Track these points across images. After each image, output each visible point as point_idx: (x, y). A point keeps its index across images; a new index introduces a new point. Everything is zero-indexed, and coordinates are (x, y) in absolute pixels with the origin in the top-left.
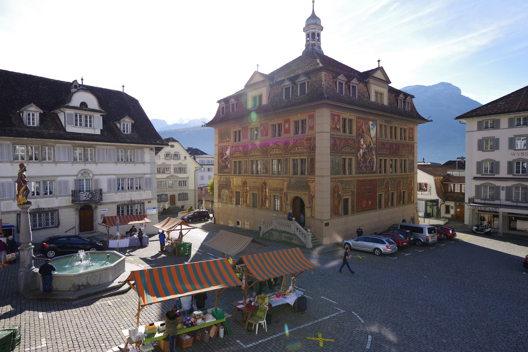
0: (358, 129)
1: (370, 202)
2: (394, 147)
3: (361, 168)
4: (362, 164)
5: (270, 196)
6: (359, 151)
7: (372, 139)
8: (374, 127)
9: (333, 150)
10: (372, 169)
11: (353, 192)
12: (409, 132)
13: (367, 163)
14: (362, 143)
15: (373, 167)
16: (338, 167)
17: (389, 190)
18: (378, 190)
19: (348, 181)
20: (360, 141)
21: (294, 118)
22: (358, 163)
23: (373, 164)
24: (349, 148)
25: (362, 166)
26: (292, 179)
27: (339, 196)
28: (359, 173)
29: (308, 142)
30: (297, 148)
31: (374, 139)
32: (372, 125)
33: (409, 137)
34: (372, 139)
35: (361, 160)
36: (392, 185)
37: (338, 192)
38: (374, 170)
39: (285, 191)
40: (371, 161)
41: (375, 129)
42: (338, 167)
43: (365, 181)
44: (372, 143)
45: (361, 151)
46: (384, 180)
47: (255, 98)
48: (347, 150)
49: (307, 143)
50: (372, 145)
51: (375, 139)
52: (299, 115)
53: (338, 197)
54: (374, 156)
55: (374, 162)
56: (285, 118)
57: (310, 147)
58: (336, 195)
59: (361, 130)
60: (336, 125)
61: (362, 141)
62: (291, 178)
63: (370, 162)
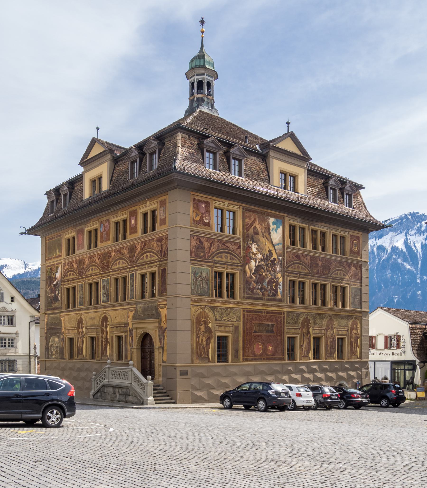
0: (246, 227)
1: (270, 348)
2: (320, 263)
4: (253, 285)
5: (112, 337)
6: (248, 262)
7: (273, 245)
8: (278, 227)
9: (197, 256)
10: (275, 294)
11: (237, 328)
12: (352, 243)
14: (254, 250)
15: (276, 291)
16: (207, 284)
17: (308, 333)
18: (286, 330)
19: (227, 309)
20: (249, 248)
21: (142, 209)
22: (247, 282)
23: (276, 286)
24: (229, 255)
26: (138, 306)
27: (208, 330)
28: (249, 298)
29: (159, 243)
30: (145, 255)
32: (274, 223)
33: (352, 251)
34: (273, 245)
35: (251, 277)
37: (206, 323)
38: (279, 296)
39: (130, 326)
40: (273, 282)
41: (280, 230)
42: (207, 284)
43: (260, 311)
44: (273, 252)
46: (299, 315)
47: (93, 182)
48: (224, 259)
49: (158, 246)
50: (275, 256)
51: (281, 246)
52: (148, 203)
53: (205, 332)
54: (279, 275)
55: (277, 284)
56: (130, 210)
57: (161, 251)
58: (202, 328)
59: (251, 230)
60: (202, 218)
62: (136, 304)
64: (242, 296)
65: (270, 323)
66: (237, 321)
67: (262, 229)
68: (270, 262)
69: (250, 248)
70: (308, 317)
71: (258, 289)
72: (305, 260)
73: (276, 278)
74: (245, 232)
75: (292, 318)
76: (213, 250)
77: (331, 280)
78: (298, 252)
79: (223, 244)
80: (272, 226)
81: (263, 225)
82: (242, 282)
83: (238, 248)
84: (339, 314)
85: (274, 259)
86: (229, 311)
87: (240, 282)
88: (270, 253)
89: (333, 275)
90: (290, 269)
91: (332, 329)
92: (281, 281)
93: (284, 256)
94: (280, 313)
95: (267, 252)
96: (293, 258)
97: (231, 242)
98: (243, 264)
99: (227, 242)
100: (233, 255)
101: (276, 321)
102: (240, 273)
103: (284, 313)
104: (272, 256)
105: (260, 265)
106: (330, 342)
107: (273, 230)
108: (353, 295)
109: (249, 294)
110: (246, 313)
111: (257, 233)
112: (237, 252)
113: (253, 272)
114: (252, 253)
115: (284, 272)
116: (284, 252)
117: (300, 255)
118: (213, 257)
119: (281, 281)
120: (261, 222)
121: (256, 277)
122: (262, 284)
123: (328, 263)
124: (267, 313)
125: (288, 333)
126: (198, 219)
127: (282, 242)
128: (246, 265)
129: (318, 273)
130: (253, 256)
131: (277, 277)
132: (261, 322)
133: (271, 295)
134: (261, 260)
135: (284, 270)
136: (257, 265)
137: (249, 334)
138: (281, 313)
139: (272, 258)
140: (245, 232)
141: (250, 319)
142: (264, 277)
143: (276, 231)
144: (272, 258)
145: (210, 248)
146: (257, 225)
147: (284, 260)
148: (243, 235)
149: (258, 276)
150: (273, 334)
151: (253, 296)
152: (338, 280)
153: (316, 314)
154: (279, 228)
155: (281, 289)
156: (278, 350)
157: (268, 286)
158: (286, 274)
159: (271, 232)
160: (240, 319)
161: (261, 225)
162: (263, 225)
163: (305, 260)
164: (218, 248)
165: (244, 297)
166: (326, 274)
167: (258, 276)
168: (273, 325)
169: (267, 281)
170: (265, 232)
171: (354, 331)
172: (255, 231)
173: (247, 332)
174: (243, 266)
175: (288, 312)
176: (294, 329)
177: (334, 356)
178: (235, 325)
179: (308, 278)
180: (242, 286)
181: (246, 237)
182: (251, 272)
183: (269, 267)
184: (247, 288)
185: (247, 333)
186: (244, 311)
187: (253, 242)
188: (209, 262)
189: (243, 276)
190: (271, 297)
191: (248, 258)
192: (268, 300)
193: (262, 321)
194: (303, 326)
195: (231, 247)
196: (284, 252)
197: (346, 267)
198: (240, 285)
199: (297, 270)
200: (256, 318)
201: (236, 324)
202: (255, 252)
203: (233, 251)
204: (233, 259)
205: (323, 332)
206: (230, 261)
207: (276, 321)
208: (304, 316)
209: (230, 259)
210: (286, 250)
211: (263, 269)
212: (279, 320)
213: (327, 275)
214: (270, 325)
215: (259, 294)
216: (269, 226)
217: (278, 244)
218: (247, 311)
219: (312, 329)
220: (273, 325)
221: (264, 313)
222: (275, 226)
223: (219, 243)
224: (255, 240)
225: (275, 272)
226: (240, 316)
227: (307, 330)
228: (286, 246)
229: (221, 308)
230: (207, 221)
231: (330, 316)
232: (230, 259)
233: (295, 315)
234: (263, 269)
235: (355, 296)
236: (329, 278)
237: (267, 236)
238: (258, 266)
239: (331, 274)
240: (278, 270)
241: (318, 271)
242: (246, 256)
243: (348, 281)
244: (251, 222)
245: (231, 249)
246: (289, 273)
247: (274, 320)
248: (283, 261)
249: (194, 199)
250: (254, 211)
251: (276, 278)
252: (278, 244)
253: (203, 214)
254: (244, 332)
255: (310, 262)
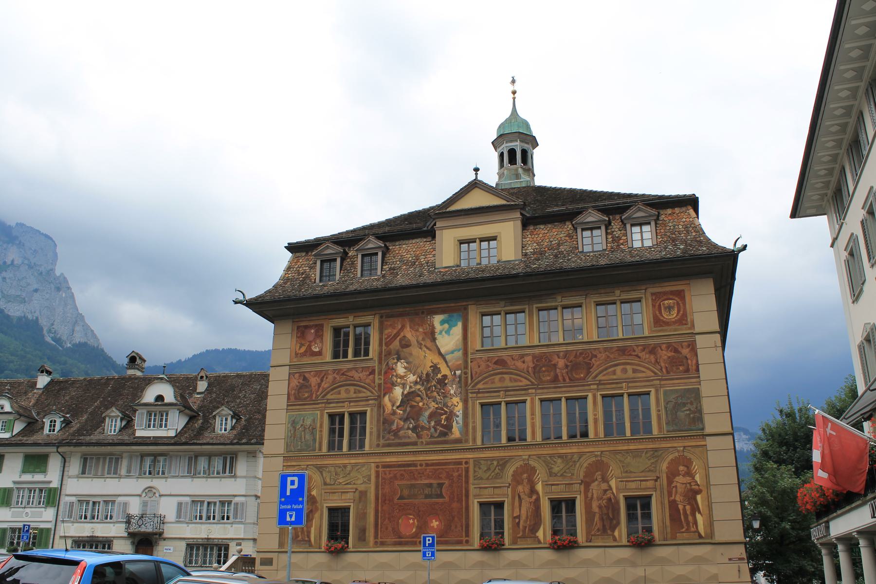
2: (561, 363)
3: (396, 433)
4: (397, 423)
13: (424, 420)
15: (449, 427)
17: (533, 491)
19: (345, 466)
20: (390, 369)
22: (385, 422)
24: (352, 389)
25: (399, 429)
28: (389, 445)
31: (455, 358)
32: (442, 322)
36: (551, 474)
41: (458, 329)
45: (398, 392)
48: (344, 395)
50: (445, 371)
51: (460, 354)
54: (456, 400)
55: (451, 416)
59: (396, 343)
60: (310, 346)
61: (400, 369)
63: (431, 416)
64: (375, 442)
65: (434, 482)
66: (364, 482)
67: (418, 337)
68: (434, 383)
69: (393, 369)
70: (531, 463)
71: (408, 428)
72: (519, 364)
73: (447, 407)
74: (384, 347)
75: (489, 469)
76: (325, 386)
77: (595, 387)
78: (500, 354)
79: (343, 374)
80: (438, 327)
81: (421, 330)
82: (375, 422)
83: (371, 374)
84: (626, 448)
85: (445, 377)
86: (349, 468)
87: (371, 423)
88: (433, 371)
89: (599, 378)
90: (480, 386)
91: (605, 480)
92: (459, 410)
93: (466, 367)
94: (458, 463)
95: (429, 369)
96: (488, 366)
97: (356, 369)
98: (379, 396)
99: (349, 370)
100: (359, 386)
101: (449, 476)
102: (372, 410)
103: (466, 463)
104: (439, 371)
105: (413, 392)
106: (600, 507)
107: (441, 332)
108: (670, 406)
109: (389, 439)
110: (380, 469)
111: (406, 345)
112: (368, 381)
113: (398, 404)
114: (397, 376)
115: (467, 394)
116: (466, 361)
117: (505, 358)
118: (325, 395)
119: (459, 410)
120: (417, 327)
121: (404, 411)
122: (417, 419)
123: (584, 358)
124: (427, 465)
125: (476, 496)
126: (303, 349)
127: (461, 346)
128: (384, 395)
129: (555, 379)
130: (399, 380)
131: (449, 404)
132: (413, 482)
133: (436, 435)
134: (416, 383)
135: (467, 390)
136: (406, 392)
137: (387, 502)
138: (460, 463)
139: (439, 376)
140: (384, 347)
141: (391, 478)
142: (421, 409)
143: (448, 332)
144: (439, 376)
145: (319, 385)
146: (409, 333)
147: (466, 373)
148: (380, 353)
149: (408, 409)
150: (441, 500)
151: (397, 441)
152: (617, 383)
153: (552, 456)
154: (456, 325)
155: (461, 422)
156: (453, 528)
157: (429, 422)
158: (470, 395)
159: (437, 336)
160: (369, 480)
161: (417, 330)
162: (421, 330)
163: (519, 364)
164: (334, 383)
165: (378, 445)
166: (581, 379)
167: (408, 409)
168: (443, 484)
169: (427, 414)
170: (423, 339)
171: (680, 479)
172: (403, 343)
173: (382, 500)
174: (379, 399)
175: (477, 462)
176: (494, 487)
177: (616, 533)
178: (360, 489)
179: (528, 394)
180: (375, 429)
181: (385, 355)
182: (393, 406)
183: (432, 391)
184: (384, 430)
185: (384, 501)
186: (377, 467)
187: (399, 359)
188: (318, 404)
189: (379, 415)
190: (438, 437)
191: (389, 385)
192: (428, 444)
193: (416, 479)
194: (517, 479)
195: (356, 375)
196: (466, 361)
197: (640, 354)
198: (371, 428)
199: (498, 385)
200: (401, 475)
201: (362, 488)
202: (402, 374)
203: (360, 381)
204: (360, 392)
205: (576, 487)
206: (354, 396)
207: (449, 476)
208: (521, 463)
209: (355, 393)
210: (470, 356)
211: (419, 396)
212: (456, 474)
213: (584, 379)
214: (435, 485)
215: (409, 437)
216: (433, 328)
217: (452, 352)
218: (384, 466)
219: (545, 485)
220: (441, 485)
221: (421, 465)
222: (446, 326)
223: (335, 375)
224: (402, 354)
225: (444, 397)
226: (370, 476)
227: (528, 487)
228: (470, 351)
229: (336, 466)
230: (317, 350)
231: (596, 456)
232: (355, 393)
233: (495, 463)
234: (419, 396)
235: (677, 406)
236: (589, 385)
237: (429, 343)
238: (409, 393)
239: (596, 376)
240: (452, 392)
241: (556, 376)
242: (385, 383)
243: (653, 380)
244: (395, 332)
245: (357, 379)
246: (479, 392)
247: (443, 475)
248: (463, 376)
249: (298, 327)
250: (401, 315)
251: (447, 407)
252: (452, 352)
253: (311, 342)
254: (377, 498)
255: (531, 365)
